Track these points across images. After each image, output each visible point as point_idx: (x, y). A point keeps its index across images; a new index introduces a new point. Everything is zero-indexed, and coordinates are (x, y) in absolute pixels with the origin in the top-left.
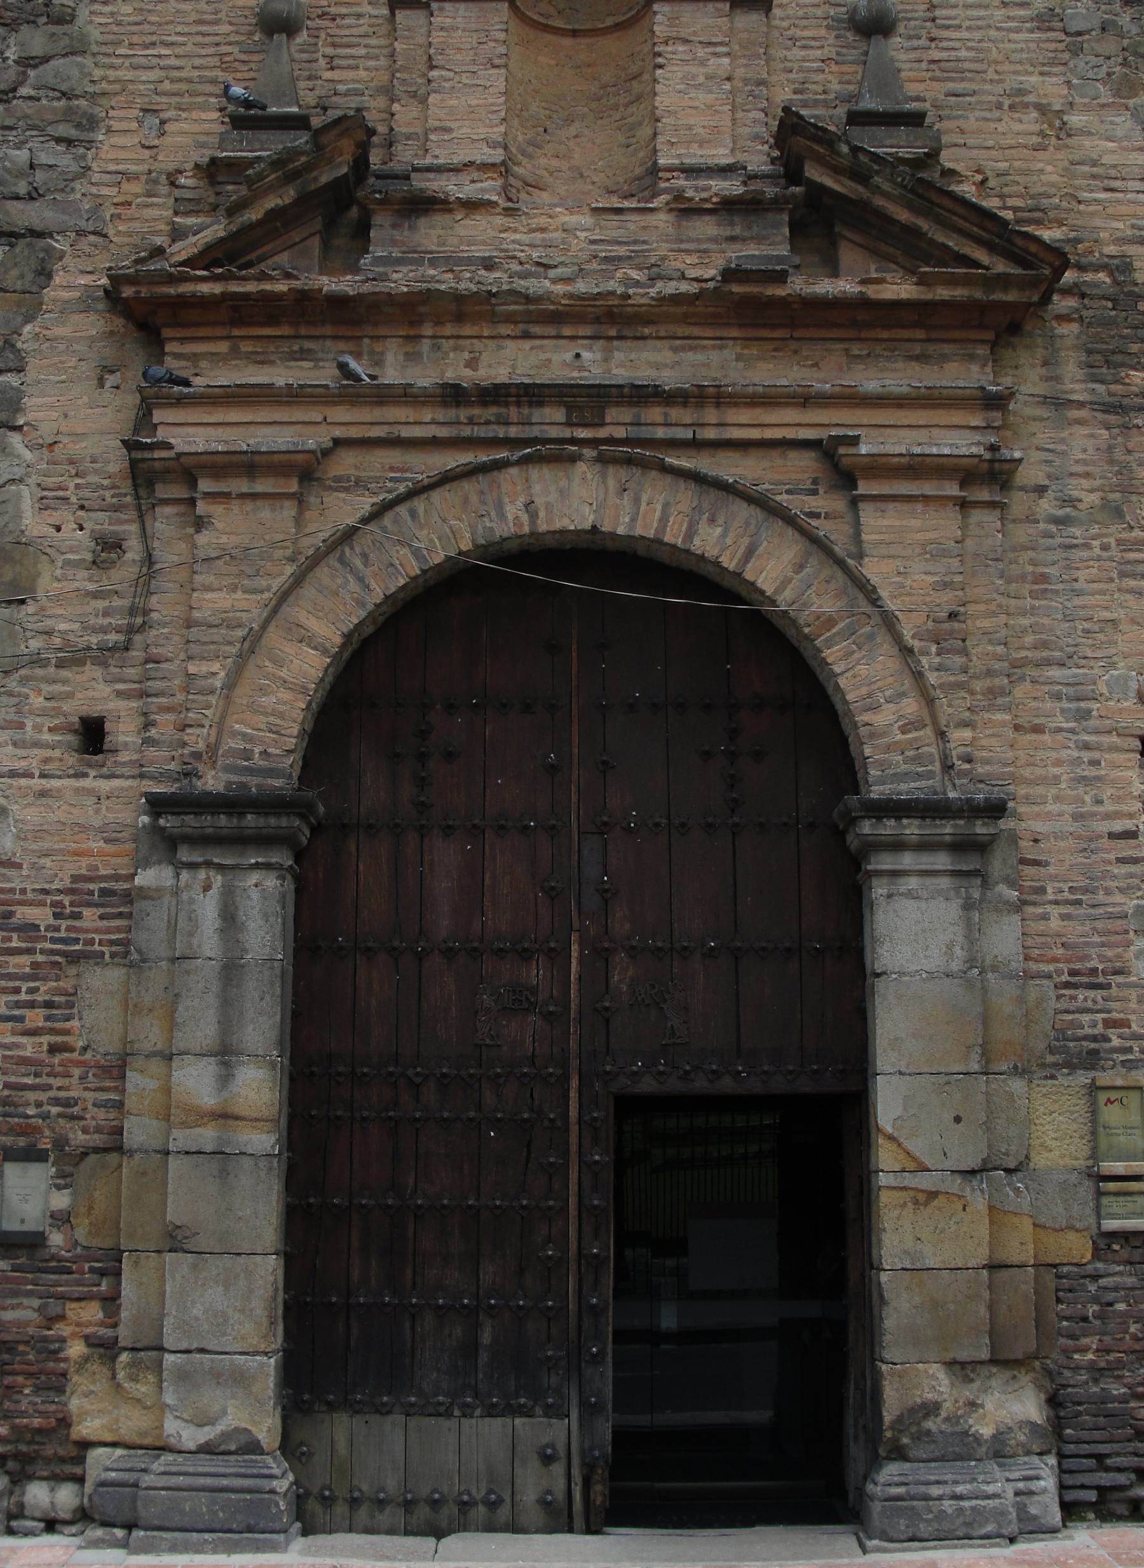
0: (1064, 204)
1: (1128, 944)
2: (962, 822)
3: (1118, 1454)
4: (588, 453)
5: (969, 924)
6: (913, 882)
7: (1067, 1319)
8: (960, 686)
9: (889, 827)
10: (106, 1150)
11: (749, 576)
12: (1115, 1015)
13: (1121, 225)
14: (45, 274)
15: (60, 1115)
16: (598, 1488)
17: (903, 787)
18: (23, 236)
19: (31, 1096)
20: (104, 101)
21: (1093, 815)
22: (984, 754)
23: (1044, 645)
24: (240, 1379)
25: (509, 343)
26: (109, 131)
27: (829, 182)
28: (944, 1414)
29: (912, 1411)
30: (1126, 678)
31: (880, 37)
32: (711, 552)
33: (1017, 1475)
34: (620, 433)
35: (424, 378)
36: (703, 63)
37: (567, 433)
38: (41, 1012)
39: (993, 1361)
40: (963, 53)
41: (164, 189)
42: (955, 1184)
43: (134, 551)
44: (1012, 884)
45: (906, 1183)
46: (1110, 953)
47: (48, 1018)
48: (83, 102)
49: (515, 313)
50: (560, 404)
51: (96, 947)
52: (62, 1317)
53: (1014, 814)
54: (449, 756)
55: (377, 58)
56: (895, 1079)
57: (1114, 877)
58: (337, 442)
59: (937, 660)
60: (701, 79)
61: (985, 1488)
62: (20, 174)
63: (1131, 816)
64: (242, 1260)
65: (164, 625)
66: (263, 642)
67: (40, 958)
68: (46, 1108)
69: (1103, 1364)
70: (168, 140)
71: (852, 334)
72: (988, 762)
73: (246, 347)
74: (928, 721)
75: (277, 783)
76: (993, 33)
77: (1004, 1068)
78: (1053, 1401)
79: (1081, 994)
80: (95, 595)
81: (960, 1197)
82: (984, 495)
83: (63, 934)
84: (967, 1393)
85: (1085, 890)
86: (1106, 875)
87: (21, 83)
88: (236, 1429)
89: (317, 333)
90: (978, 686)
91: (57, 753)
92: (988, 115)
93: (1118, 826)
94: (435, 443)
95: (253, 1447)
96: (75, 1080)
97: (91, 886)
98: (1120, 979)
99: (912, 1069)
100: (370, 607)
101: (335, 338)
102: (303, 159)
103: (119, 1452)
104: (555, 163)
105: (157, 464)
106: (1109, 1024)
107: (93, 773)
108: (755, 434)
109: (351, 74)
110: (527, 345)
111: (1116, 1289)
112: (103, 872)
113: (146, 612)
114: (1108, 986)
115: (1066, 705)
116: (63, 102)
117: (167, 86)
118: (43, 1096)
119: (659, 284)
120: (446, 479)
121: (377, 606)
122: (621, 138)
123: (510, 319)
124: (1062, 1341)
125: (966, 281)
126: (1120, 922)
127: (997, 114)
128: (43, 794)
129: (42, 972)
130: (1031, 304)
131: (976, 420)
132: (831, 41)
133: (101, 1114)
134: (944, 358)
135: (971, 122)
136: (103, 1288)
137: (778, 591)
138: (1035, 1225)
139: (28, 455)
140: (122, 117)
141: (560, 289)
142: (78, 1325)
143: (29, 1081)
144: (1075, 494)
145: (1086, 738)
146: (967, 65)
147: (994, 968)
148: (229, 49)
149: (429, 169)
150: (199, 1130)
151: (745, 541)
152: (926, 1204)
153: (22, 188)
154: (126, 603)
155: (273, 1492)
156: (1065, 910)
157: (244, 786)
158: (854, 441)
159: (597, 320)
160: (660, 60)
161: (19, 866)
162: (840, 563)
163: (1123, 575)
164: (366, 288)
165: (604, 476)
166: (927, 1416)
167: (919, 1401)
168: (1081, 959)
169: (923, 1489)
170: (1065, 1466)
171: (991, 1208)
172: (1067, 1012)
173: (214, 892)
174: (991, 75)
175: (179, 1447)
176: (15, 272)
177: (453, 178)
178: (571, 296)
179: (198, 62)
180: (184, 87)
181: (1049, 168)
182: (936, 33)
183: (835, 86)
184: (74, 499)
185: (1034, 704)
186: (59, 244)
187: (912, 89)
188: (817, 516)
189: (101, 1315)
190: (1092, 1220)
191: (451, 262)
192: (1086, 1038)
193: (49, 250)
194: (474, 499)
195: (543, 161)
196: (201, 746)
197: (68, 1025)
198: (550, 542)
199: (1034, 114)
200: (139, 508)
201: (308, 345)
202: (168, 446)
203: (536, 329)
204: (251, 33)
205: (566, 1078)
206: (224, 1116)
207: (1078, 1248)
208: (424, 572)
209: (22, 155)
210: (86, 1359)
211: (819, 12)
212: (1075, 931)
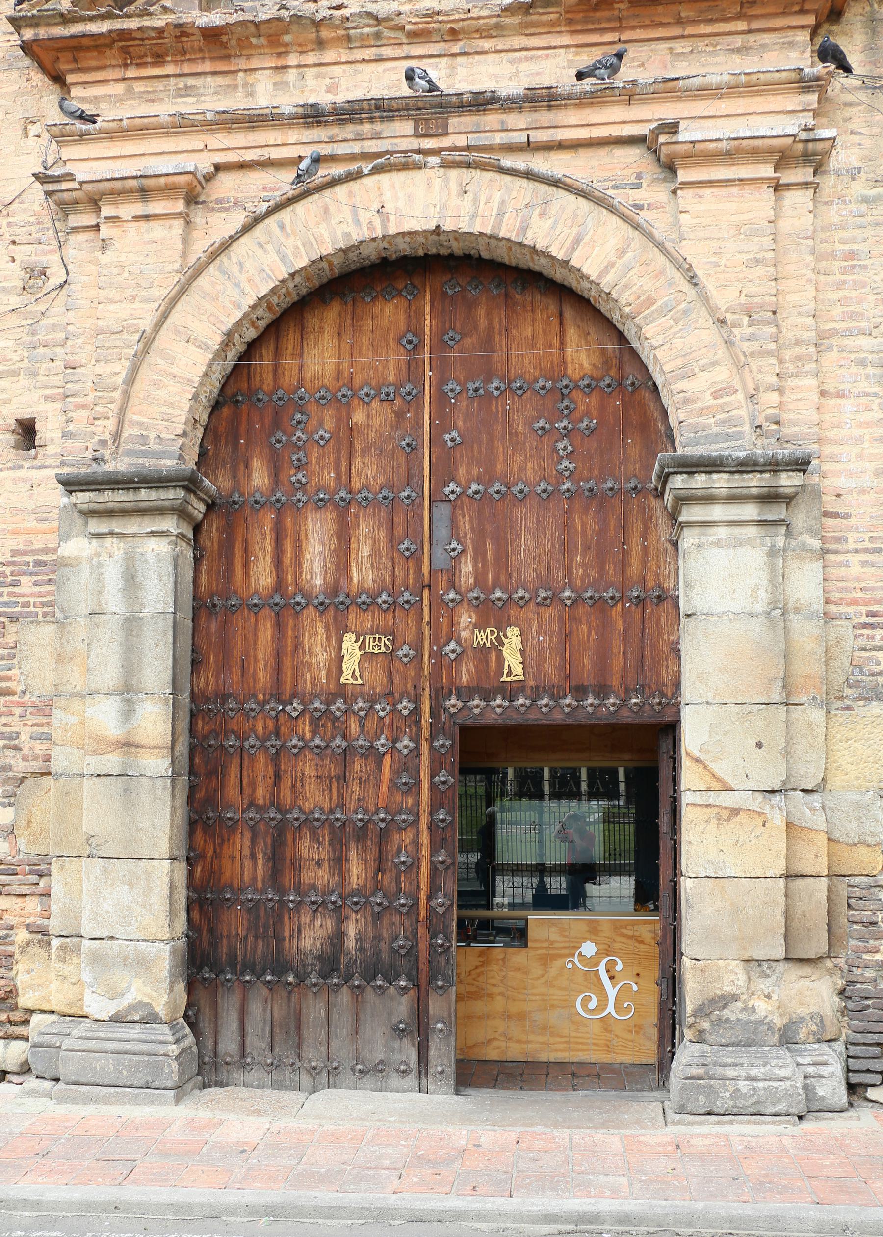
2: (767, 475)
4: (434, 160)
5: (773, 570)
6: (722, 532)
8: (769, 353)
17: (714, 447)
22: (792, 416)
24: (142, 964)
29: (712, 1001)
35: (287, 104)
37: (415, 144)
42: (756, 803)
44: (811, 531)
45: (711, 801)
51: (32, 609)
56: (703, 709)
58: (218, 168)
59: (749, 330)
61: (776, 1071)
64: (142, 863)
65: (77, 336)
66: (156, 343)
71: (677, 31)
73: (139, 87)
74: (738, 386)
77: (803, 699)
81: (760, 814)
88: (140, 1002)
89: (199, 70)
90: (787, 354)
95: (151, 1019)
99: (718, 700)
100: (245, 308)
101: (214, 73)
112: (36, 546)
124: (852, 942)
137: (600, 276)
138: (829, 839)
147: (797, 610)
152: (729, 820)
156: (869, 557)
167: (719, 993)
172: (865, 650)
196: (107, 436)
197: (10, 673)
201: (191, 81)
208: (292, 275)
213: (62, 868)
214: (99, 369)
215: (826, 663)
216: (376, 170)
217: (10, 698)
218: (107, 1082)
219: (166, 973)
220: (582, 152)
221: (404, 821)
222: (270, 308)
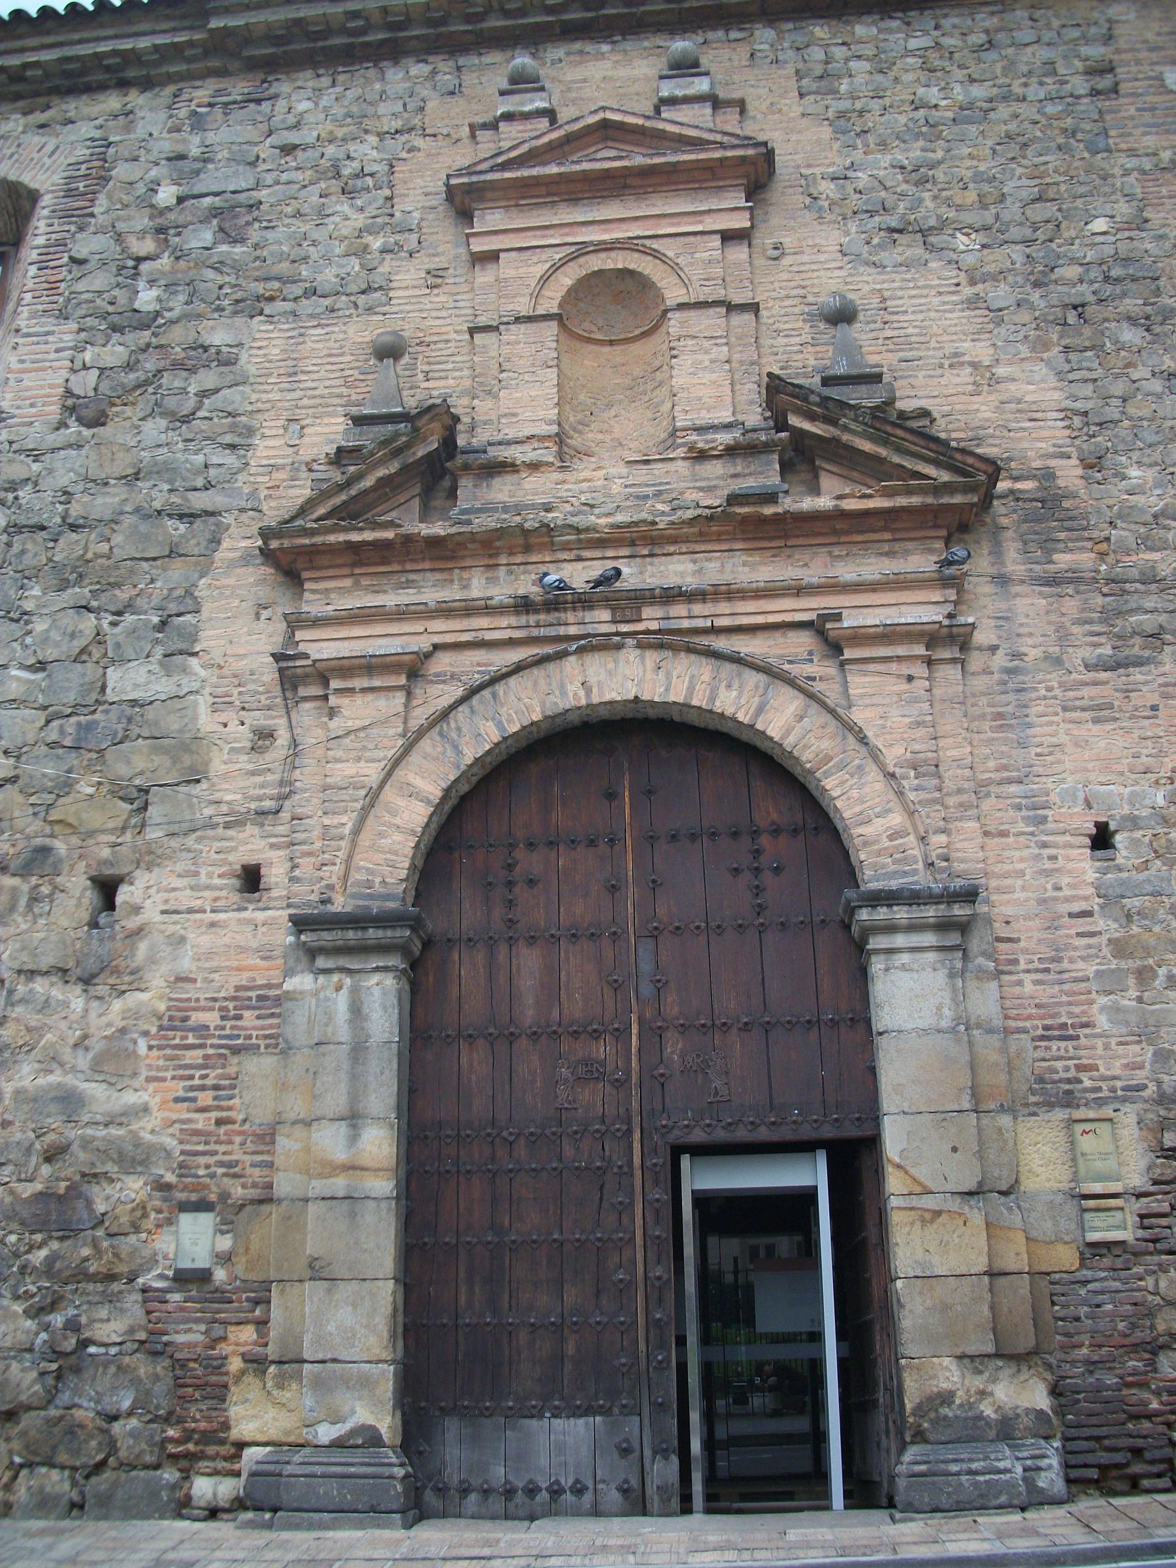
0: (997, 433)
1: (1091, 1002)
2: (942, 907)
3: (1114, 1436)
4: (630, 642)
5: (954, 990)
6: (905, 958)
7: (1061, 1319)
8: (934, 801)
9: (882, 913)
10: (261, 1202)
11: (759, 726)
12: (1085, 1061)
13: (1043, 445)
14: (215, 541)
15: (225, 1175)
16: (711, 1538)
18: (200, 516)
19: (202, 1160)
20: (259, 416)
21: (1055, 899)
22: (959, 854)
23: (1005, 768)
24: (365, 1383)
25: (565, 565)
26: (263, 436)
27: (807, 426)
28: (958, 1401)
29: (930, 1399)
30: (1075, 789)
31: (845, 325)
32: (729, 712)
33: (1025, 1454)
34: (654, 626)
36: (706, 352)
37: (612, 628)
38: (210, 1094)
39: (998, 1355)
40: (910, 331)
41: (304, 474)
42: (955, 1204)
43: (283, 738)
45: (914, 1204)
46: (1076, 1010)
47: (215, 1098)
48: (243, 419)
49: (569, 542)
50: (606, 607)
51: (254, 1041)
52: (224, 1339)
53: (987, 901)
54: (531, 882)
55: (461, 370)
56: (899, 1118)
57: (1075, 948)
58: (436, 647)
60: (707, 363)
61: (997, 1464)
62: (198, 473)
63: (1086, 898)
67: (211, 1051)
68: (213, 1169)
69: (1096, 1358)
70: (306, 440)
72: (963, 861)
73: (365, 582)
74: (910, 830)
75: (392, 905)
76: (932, 314)
77: (992, 1107)
78: (1055, 1391)
79: (1054, 1045)
80: (253, 773)
81: (960, 1214)
82: (947, 654)
83: (228, 1032)
84: (978, 1382)
85: (1053, 960)
86: (1068, 947)
87: (199, 409)
90: (951, 801)
91: (224, 893)
92: (932, 373)
93: (1076, 907)
94: (511, 643)
96: (236, 1146)
97: (250, 994)
98: (1087, 1031)
99: (914, 1109)
100: (463, 768)
102: (404, 439)
103: (268, 1449)
104: (600, 436)
105: (299, 671)
106: (1079, 1068)
107: (251, 907)
108: (760, 620)
109: (442, 383)
110: (580, 565)
111: (1102, 1292)
112: (260, 982)
113: (291, 784)
114: (1077, 1038)
115: (1024, 813)
116: (230, 419)
117: (305, 402)
118: (211, 1160)
119: (679, 513)
120: (518, 668)
121: (470, 766)
122: (649, 415)
123: (566, 547)
125: (920, 490)
126: (1084, 985)
127: (939, 372)
128: (213, 924)
129: (211, 1062)
130: (973, 505)
131: (937, 596)
132: (807, 329)
133: (257, 1172)
134: (907, 552)
135: (920, 378)
136: (257, 1312)
139: (203, 673)
140: (271, 425)
141: (603, 521)
142: (237, 1344)
143: (200, 1148)
144: (1024, 649)
145: (1045, 838)
146: (913, 339)
147: (978, 1026)
148: (350, 372)
149: (500, 443)
150: (332, 1180)
151: (757, 700)
152: (932, 1222)
153: (200, 482)
154: (277, 777)
155: (391, 1477)
156: (1039, 976)
157: (368, 907)
158: (838, 617)
159: (633, 543)
160: (674, 352)
161: (194, 981)
162: (832, 712)
163: (1065, 709)
164: (454, 530)
165: (643, 658)
166: (942, 1403)
167: (935, 1390)
168: (1053, 1016)
169: (943, 1466)
170: (1069, 1449)
171: (988, 1225)
172: (1044, 1060)
173: (344, 992)
174: (933, 344)
175: (315, 1442)
176: (194, 542)
177: (519, 448)
178: (612, 526)
179: (328, 383)
180: (319, 401)
181: (983, 408)
182: (887, 317)
183: (812, 362)
184: (237, 703)
185: (999, 814)
186: (228, 519)
187: (873, 359)
188: (813, 679)
189: (255, 1336)
190: (1078, 1233)
191: (518, 509)
192: (1060, 1081)
193: (218, 525)
194: (542, 682)
195: (590, 435)
196: (334, 880)
197: (231, 1102)
198: (604, 713)
199: (969, 370)
200: (287, 706)
201: (412, 577)
202: (306, 656)
203: (587, 554)
204: (367, 360)
205: (630, 1131)
206: (351, 1168)
207: (1066, 1257)
208: (505, 739)
209: (199, 459)
210: (243, 1372)
211: (797, 310)
212: (1045, 994)
213: (282, 1291)
214: (327, 821)
215: (1010, 1073)
216: (580, 651)
217: (230, 1127)
218: (332, 1507)
219: (390, 1394)
220: (759, 634)
221: (621, 1239)
222: (483, 767)
